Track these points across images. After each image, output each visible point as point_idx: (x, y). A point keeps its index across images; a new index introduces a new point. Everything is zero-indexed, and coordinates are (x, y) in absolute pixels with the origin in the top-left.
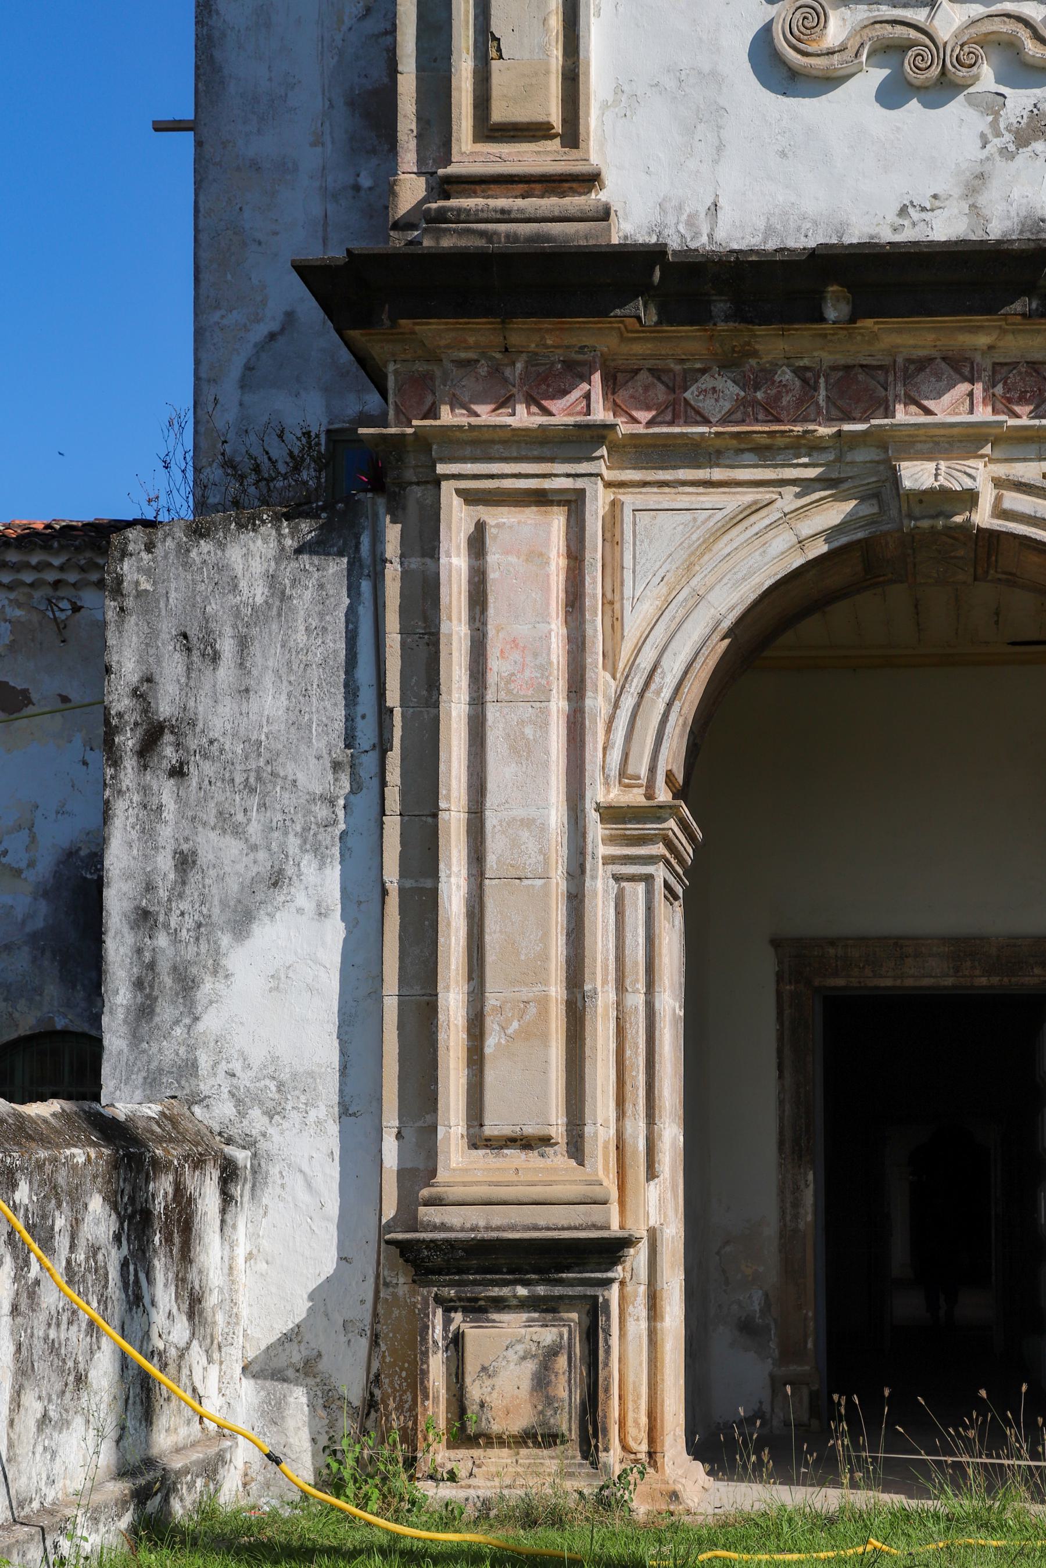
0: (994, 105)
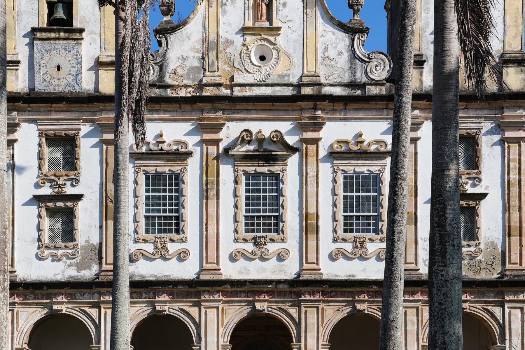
0: (65, 262)
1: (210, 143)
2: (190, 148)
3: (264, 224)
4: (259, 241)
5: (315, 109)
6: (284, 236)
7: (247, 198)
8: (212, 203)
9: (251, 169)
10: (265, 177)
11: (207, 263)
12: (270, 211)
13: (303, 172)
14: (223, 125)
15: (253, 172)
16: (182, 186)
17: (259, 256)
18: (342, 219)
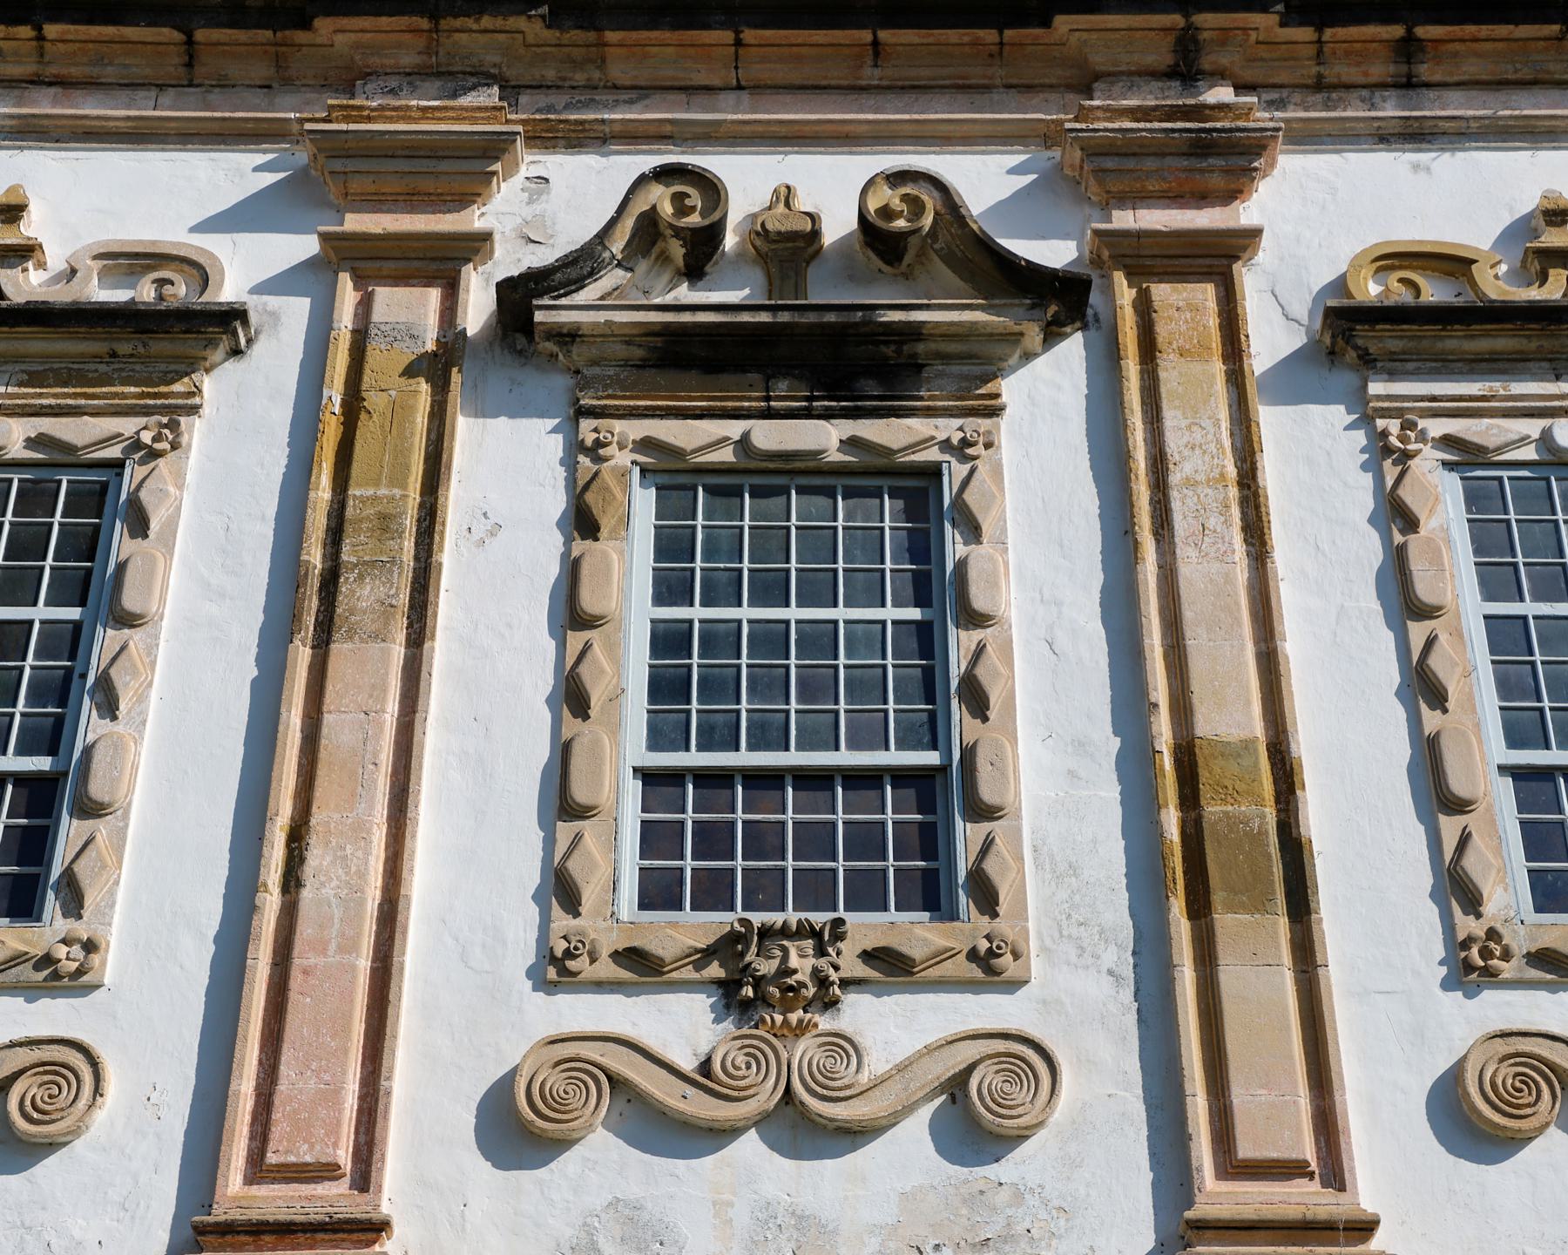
1: (389, 266)
2: (229, 292)
3: (816, 840)
4: (766, 967)
5: (1186, 68)
6: (1002, 925)
7: (669, 640)
8: (366, 669)
9: (705, 437)
10: (822, 502)
11: (258, 1170)
12: (869, 735)
13: (1123, 458)
14: (494, 149)
15: (726, 455)
16: (121, 544)
17: (766, 1097)
18: (1502, 797)
